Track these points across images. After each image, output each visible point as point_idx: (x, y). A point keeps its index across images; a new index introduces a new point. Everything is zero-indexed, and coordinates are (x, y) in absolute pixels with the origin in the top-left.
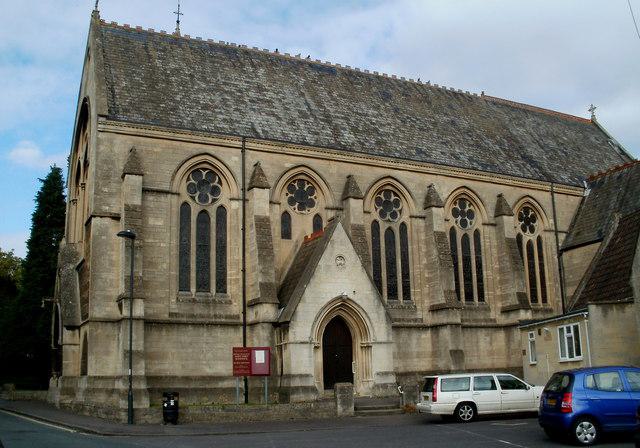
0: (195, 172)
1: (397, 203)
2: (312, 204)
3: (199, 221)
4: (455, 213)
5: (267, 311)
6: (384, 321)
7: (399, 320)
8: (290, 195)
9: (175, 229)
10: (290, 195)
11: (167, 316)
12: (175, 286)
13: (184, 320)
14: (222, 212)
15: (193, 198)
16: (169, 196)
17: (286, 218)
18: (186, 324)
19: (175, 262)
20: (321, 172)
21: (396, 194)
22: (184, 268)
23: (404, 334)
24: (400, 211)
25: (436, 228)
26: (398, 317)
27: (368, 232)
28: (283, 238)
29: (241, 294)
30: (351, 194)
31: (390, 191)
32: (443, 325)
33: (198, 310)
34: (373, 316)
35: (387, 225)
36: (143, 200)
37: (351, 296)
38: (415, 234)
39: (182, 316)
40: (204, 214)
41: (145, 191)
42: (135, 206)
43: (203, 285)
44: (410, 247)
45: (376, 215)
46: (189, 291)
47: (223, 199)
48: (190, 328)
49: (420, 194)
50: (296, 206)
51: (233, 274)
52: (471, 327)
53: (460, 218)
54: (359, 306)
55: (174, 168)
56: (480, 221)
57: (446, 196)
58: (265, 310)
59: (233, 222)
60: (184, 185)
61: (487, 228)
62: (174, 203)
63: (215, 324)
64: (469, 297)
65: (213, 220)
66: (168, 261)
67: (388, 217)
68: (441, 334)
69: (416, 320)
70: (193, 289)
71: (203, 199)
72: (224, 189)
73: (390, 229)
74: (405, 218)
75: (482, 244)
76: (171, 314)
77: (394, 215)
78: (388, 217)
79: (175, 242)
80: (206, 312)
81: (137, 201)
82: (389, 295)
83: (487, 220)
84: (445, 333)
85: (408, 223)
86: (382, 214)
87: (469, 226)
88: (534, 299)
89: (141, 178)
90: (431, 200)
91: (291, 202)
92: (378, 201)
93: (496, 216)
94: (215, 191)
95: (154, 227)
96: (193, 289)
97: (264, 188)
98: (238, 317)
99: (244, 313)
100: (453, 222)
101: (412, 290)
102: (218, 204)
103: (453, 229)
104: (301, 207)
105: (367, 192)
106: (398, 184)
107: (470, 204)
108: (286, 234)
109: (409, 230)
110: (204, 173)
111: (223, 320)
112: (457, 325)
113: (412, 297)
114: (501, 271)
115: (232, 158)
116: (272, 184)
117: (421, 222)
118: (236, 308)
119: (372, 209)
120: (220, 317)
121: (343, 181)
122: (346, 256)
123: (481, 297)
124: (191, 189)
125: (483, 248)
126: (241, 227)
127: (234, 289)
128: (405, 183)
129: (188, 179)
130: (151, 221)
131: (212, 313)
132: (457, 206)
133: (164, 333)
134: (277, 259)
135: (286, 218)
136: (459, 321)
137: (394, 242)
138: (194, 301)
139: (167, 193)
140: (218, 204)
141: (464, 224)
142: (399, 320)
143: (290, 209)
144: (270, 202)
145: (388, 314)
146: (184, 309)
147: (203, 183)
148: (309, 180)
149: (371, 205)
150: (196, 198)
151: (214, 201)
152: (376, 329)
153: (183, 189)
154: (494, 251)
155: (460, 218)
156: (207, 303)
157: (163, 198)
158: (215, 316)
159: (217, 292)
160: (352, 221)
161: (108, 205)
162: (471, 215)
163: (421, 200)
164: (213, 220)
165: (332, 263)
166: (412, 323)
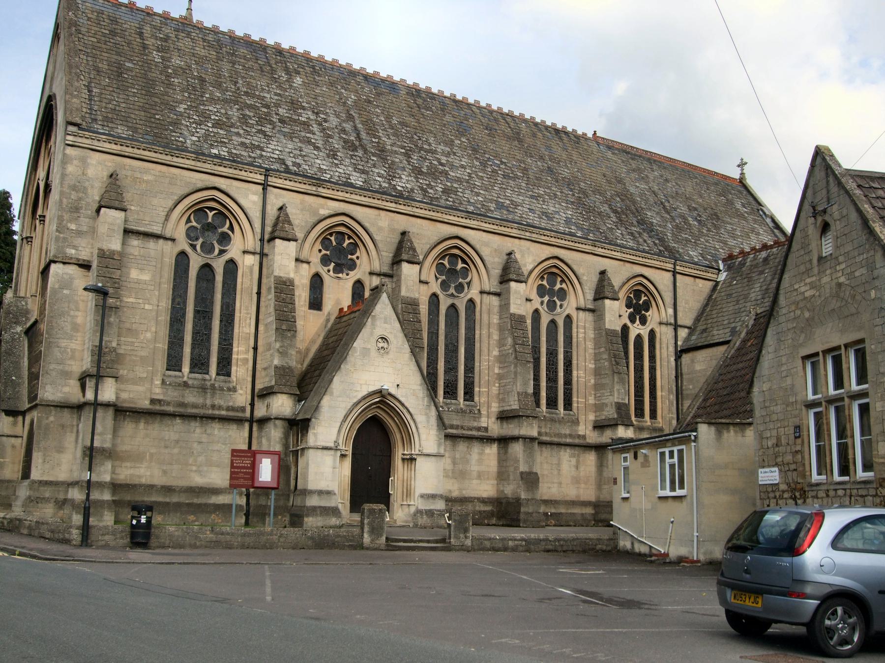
0: (199, 211)
1: (465, 272)
2: (352, 266)
3: (199, 278)
4: (541, 291)
5: (282, 405)
6: (435, 427)
7: (457, 427)
8: (324, 252)
9: (167, 287)
10: (324, 252)
11: (147, 402)
12: (161, 363)
13: (170, 409)
14: (231, 267)
15: (194, 247)
16: (161, 241)
17: (317, 282)
18: (173, 415)
19: (164, 332)
20: (367, 225)
21: (464, 261)
23: (462, 446)
24: (469, 284)
25: (513, 309)
26: (455, 423)
27: (424, 308)
29: (250, 379)
30: (404, 256)
32: (515, 439)
33: (191, 398)
34: (420, 418)
35: (450, 301)
36: (123, 244)
37: (393, 391)
38: (485, 317)
39: (168, 404)
40: (207, 268)
41: (127, 232)
42: (113, 252)
43: (199, 364)
44: (477, 332)
46: (207, 373)
47: (234, 251)
48: (178, 421)
49: (496, 263)
51: (241, 351)
52: (551, 444)
53: (546, 299)
54: (403, 405)
55: (170, 203)
57: (530, 267)
58: (280, 402)
59: (246, 281)
60: (182, 228)
62: (169, 251)
63: (212, 418)
64: (552, 403)
65: (219, 278)
66: (153, 329)
67: (452, 290)
68: (510, 450)
69: (479, 429)
70: (186, 369)
71: (208, 248)
72: (236, 237)
73: (453, 306)
74: (473, 293)
75: (574, 335)
76: (153, 401)
77: (460, 288)
78: (452, 290)
79: (165, 304)
80: (200, 401)
81: (115, 244)
83: (582, 304)
84: (517, 449)
85: (477, 300)
86: (444, 286)
87: (558, 310)
88: (640, 413)
89: (122, 214)
91: (325, 261)
92: (440, 268)
93: (595, 300)
94: (225, 239)
95: (138, 282)
96: (186, 369)
97: (289, 240)
98: (243, 409)
99: (252, 405)
100: (536, 303)
101: (476, 389)
102: (226, 257)
103: (536, 311)
107: (563, 281)
108: (316, 304)
109: (478, 309)
111: (224, 413)
112: (532, 439)
113: (476, 399)
114: (597, 372)
115: (249, 197)
116: (300, 235)
117: (495, 300)
118: (242, 398)
119: (432, 279)
120: (220, 408)
121: (396, 238)
122: (390, 337)
123: (568, 405)
124: (191, 235)
125: (574, 340)
126: (255, 290)
127: (240, 372)
128: (478, 247)
129: (189, 221)
130: (134, 274)
131: (209, 402)
132: (545, 283)
133: (142, 425)
134: (300, 335)
135: (317, 282)
137: (458, 325)
138: (186, 385)
139: (157, 237)
140: (226, 257)
141: (552, 306)
142: (457, 427)
144: (297, 260)
145: (440, 418)
146: (172, 395)
147: (209, 227)
149: (429, 272)
150: (198, 248)
151: (222, 252)
152: (423, 437)
153: (179, 231)
154: (590, 345)
155: (546, 299)
156: (203, 389)
157: (152, 244)
158: (213, 407)
159: (218, 374)
160: (404, 293)
161: (75, 247)
162: (562, 295)
163: (496, 272)
164: (219, 278)
165: (372, 346)
166: (475, 433)
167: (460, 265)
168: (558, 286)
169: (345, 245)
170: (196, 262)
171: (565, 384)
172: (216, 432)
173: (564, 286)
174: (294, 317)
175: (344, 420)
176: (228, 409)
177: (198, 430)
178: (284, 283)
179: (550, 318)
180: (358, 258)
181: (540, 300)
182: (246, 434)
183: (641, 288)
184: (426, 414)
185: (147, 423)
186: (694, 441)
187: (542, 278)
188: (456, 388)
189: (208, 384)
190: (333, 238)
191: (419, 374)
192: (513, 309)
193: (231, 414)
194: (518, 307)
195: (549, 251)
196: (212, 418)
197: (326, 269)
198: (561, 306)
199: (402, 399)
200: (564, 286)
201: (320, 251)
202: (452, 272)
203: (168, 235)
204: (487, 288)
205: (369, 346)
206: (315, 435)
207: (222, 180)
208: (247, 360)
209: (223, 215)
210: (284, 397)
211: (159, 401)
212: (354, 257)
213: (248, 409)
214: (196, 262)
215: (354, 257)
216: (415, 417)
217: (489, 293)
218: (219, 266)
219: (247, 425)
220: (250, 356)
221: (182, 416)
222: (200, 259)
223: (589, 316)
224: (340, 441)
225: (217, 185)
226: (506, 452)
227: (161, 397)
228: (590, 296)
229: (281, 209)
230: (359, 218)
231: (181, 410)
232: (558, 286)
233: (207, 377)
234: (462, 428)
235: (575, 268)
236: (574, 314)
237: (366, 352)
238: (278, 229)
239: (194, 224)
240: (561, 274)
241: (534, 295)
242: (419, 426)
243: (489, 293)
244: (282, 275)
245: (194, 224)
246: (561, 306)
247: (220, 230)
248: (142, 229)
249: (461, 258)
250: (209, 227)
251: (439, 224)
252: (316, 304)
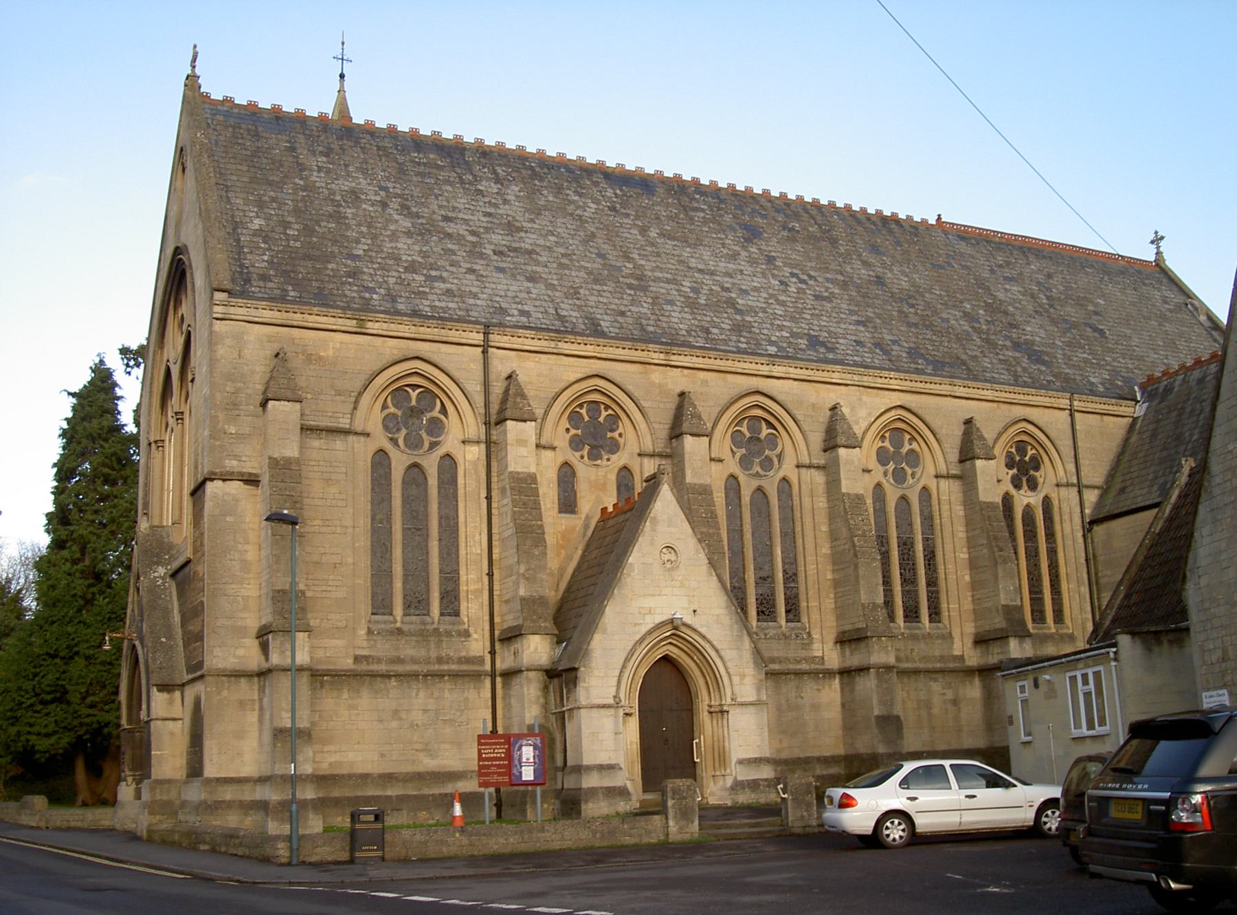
1: (772, 441)
2: (614, 447)
5: (537, 649)
8: (573, 432)
10: (573, 432)
11: (350, 661)
12: (364, 607)
13: (383, 668)
14: (449, 461)
15: (394, 441)
16: (351, 438)
17: (567, 475)
18: (387, 676)
20: (629, 388)
22: (381, 575)
23: (789, 688)
24: (780, 456)
26: (776, 654)
27: (719, 497)
28: (560, 512)
29: (487, 618)
30: (685, 426)
32: (863, 670)
35: (755, 483)
37: (688, 619)
38: (807, 502)
39: (379, 661)
41: (305, 429)
45: (733, 466)
46: (428, 614)
47: (450, 442)
50: (585, 452)
51: (471, 579)
53: (891, 466)
54: (704, 637)
57: (864, 425)
59: (470, 482)
60: (377, 416)
61: (944, 484)
62: (363, 450)
63: (440, 675)
64: (912, 614)
65: (433, 481)
68: (858, 688)
70: (398, 611)
71: (413, 443)
72: (452, 422)
76: (357, 659)
77: (767, 464)
78: (757, 468)
79: (364, 522)
80: (422, 653)
81: (292, 451)
83: (943, 469)
84: (868, 685)
85: (794, 479)
86: (745, 463)
87: (910, 481)
88: (1038, 616)
89: (298, 405)
90: (835, 435)
91: (576, 444)
92: (737, 439)
93: (961, 461)
94: (436, 427)
96: (398, 611)
98: (481, 660)
100: (878, 474)
101: (803, 604)
102: (441, 451)
103: (878, 486)
104: (594, 456)
107: (913, 439)
108: (568, 504)
110: (414, 394)
111: (454, 667)
112: (888, 668)
113: (804, 619)
114: (973, 565)
116: (539, 412)
118: (478, 645)
119: (726, 454)
120: (449, 660)
121: (672, 405)
122: (678, 546)
123: (935, 614)
124: (389, 424)
126: (484, 494)
127: (473, 608)
129: (384, 407)
131: (434, 654)
136: (891, 660)
138: (399, 631)
139: (346, 432)
140: (441, 451)
141: (899, 477)
143: (573, 457)
145: (757, 652)
146: (383, 648)
149: (722, 443)
151: (433, 445)
152: (736, 679)
155: (891, 466)
156: (423, 635)
157: (339, 444)
158: (440, 660)
159: (442, 614)
161: (237, 457)
162: (913, 458)
163: (817, 438)
164: (433, 481)
166: (804, 666)
167: (765, 431)
168: (907, 447)
169: (601, 419)
170: (399, 461)
171: (928, 585)
172: (447, 694)
173: (915, 446)
174: (541, 527)
176: (461, 661)
179: (899, 493)
180: (620, 435)
184: (738, 649)
188: (774, 606)
190: (584, 411)
193: (465, 667)
196: (440, 675)
197: (578, 454)
198: (913, 475)
199: (703, 630)
200: (915, 446)
201: (568, 430)
203: (359, 429)
206: (587, 689)
207: (426, 345)
209: (428, 396)
211: (366, 658)
212: (616, 435)
213: (488, 658)
214: (399, 461)
216: (722, 653)
217: (809, 467)
223: (955, 486)
224: (622, 695)
226: (852, 691)
228: (954, 456)
229: (509, 377)
232: (907, 447)
233: (428, 619)
236: (932, 484)
240: (909, 429)
241: (873, 463)
245: (392, 410)
246: (913, 475)
251: (729, 376)
252: (568, 504)
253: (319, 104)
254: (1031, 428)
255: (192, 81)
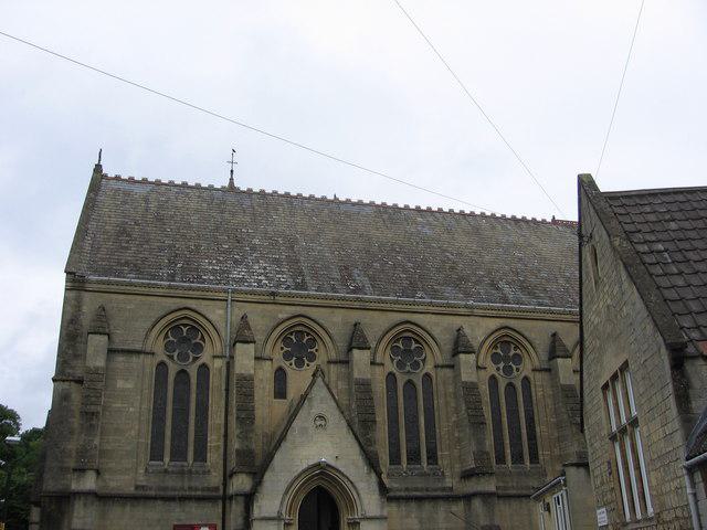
0: (175, 328)
1: (420, 350)
2: (312, 358)
3: (176, 382)
4: (496, 358)
5: (241, 483)
6: (377, 492)
7: (421, 490)
8: (285, 349)
9: (149, 393)
10: (285, 349)
11: (132, 489)
12: (144, 456)
13: (153, 493)
14: (204, 369)
15: (171, 357)
16: (142, 356)
17: (280, 375)
18: (155, 498)
19: (147, 429)
20: (321, 321)
21: (417, 342)
22: (157, 436)
23: (427, 506)
24: (424, 360)
25: (464, 378)
26: (419, 486)
27: (484, 388)
28: (275, 398)
29: (222, 462)
30: (354, 344)
31: (409, 338)
32: (474, 495)
33: (171, 482)
34: (361, 486)
35: (407, 378)
36: (108, 360)
37: (332, 463)
38: (441, 388)
39: (150, 489)
40: (183, 373)
41: (111, 351)
42: (97, 368)
43: (179, 453)
44: (436, 402)
45: (391, 367)
47: (205, 357)
48: (159, 502)
49: (446, 339)
50: (293, 361)
51: (214, 439)
52: (519, 496)
53: (501, 365)
54: (343, 475)
55: (149, 324)
56: (529, 367)
57: (481, 339)
58: (240, 481)
59: (216, 381)
60: (161, 343)
61: (539, 375)
62: (149, 364)
63: (189, 498)
64: (518, 458)
65: (194, 380)
66: (137, 427)
67: (408, 368)
68: (473, 506)
69: (444, 489)
70: (167, 459)
71: (183, 357)
72: (207, 347)
73: (183, 372)
74: (429, 368)
75: (533, 394)
76: (137, 487)
77: (416, 365)
78: (408, 368)
79: (148, 406)
80: (179, 484)
81: (100, 362)
82: (410, 460)
83: (440, 361)
84: (477, 503)
85: (433, 374)
86: (400, 365)
87: (515, 373)
88: (501, 459)
89: (252, 345)
90: (460, 345)
91: (287, 356)
92: (395, 350)
93: (550, 359)
94: (198, 348)
95: (123, 390)
96: (167, 459)
97: (247, 342)
98: (217, 489)
99: (225, 485)
100: (492, 369)
101: (439, 453)
102: (199, 362)
103: (493, 377)
104: (300, 363)
105: (481, 346)
106: (418, 329)
107: (516, 347)
108: (280, 393)
109: (434, 382)
110: (185, 330)
111: (199, 493)
112: (491, 494)
113: (440, 462)
114: (559, 426)
115: (215, 313)
116: (373, 345)
117: (448, 372)
118: (215, 479)
119: (387, 361)
120: (196, 489)
121: (348, 330)
122: (327, 415)
123: (534, 458)
124: (169, 347)
125: (534, 398)
126: (224, 388)
127: (214, 458)
128: (428, 327)
129: (166, 336)
130: (120, 384)
131: (186, 485)
132: (499, 351)
133: (128, 508)
134: (258, 421)
135: (280, 375)
136: (493, 489)
137: (416, 397)
138: (166, 471)
139: (138, 352)
140: (199, 362)
141: (508, 371)
142: (421, 490)
143: (285, 365)
144: (257, 358)
145: (381, 485)
146: (154, 481)
147: (185, 340)
148: (415, 337)
149: (383, 355)
150: (175, 358)
151: (195, 359)
152: (365, 501)
153: (159, 347)
154: (549, 401)
155: (501, 365)
156: (181, 473)
157: (134, 359)
158: (190, 488)
159: (195, 460)
160: (356, 375)
161: (72, 368)
162: (518, 359)
163: (448, 347)
164: (194, 380)
165: (310, 424)
166: (439, 493)
167: (414, 346)
168: (512, 352)
169: (304, 341)
170: (173, 369)
171: (529, 439)
172: (194, 509)
173: (518, 351)
174: (253, 407)
175: (286, 492)
176: (203, 490)
177: (178, 510)
178: (245, 378)
179: (507, 381)
180: (282, 348)
181: (495, 367)
182: (220, 511)
183: (410, 334)
184: (368, 481)
185: (132, 506)
186: (565, 485)
187: (496, 347)
188: (419, 455)
189: (186, 469)
190: (293, 337)
191: (356, 445)
192: (464, 378)
193: (206, 494)
194: (468, 375)
195: (494, 324)
196: (189, 498)
197: (288, 363)
198: (518, 370)
199: (342, 470)
200: (518, 351)
201: (282, 348)
202: (407, 352)
203: (148, 350)
204: (440, 362)
205: (306, 425)
206: (260, 507)
207: (305, 308)
208: (218, 446)
209: (195, 329)
210: (244, 476)
211: (143, 487)
212: (314, 350)
213: (221, 488)
214: (173, 369)
215: (314, 350)
216: (356, 485)
217: (442, 367)
218: (193, 371)
219: (220, 503)
220: (221, 443)
221: (163, 499)
222: (176, 367)
223: (546, 376)
224: (283, 512)
225: (189, 306)
226: (469, 509)
227: (144, 484)
228: (544, 357)
229: (356, 325)
230: (313, 317)
231: (162, 493)
232: (512, 352)
233: (186, 464)
234: (427, 490)
235: (526, 334)
236: (531, 376)
237: (304, 431)
238: (242, 335)
239: (171, 339)
240: (415, 337)
241: (489, 363)
242: (361, 492)
243: (442, 367)
244: (243, 372)
245: (171, 339)
246: (518, 370)
247: (193, 342)
248: (126, 347)
249: (415, 340)
250: (185, 340)
251: (388, 313)
252: (280, 393)
253: (221, 181)
254: (412, 326)
255: (98, 168)
